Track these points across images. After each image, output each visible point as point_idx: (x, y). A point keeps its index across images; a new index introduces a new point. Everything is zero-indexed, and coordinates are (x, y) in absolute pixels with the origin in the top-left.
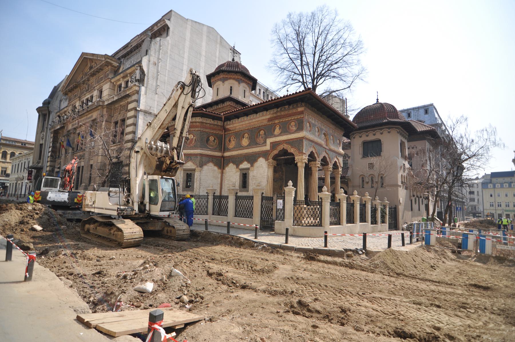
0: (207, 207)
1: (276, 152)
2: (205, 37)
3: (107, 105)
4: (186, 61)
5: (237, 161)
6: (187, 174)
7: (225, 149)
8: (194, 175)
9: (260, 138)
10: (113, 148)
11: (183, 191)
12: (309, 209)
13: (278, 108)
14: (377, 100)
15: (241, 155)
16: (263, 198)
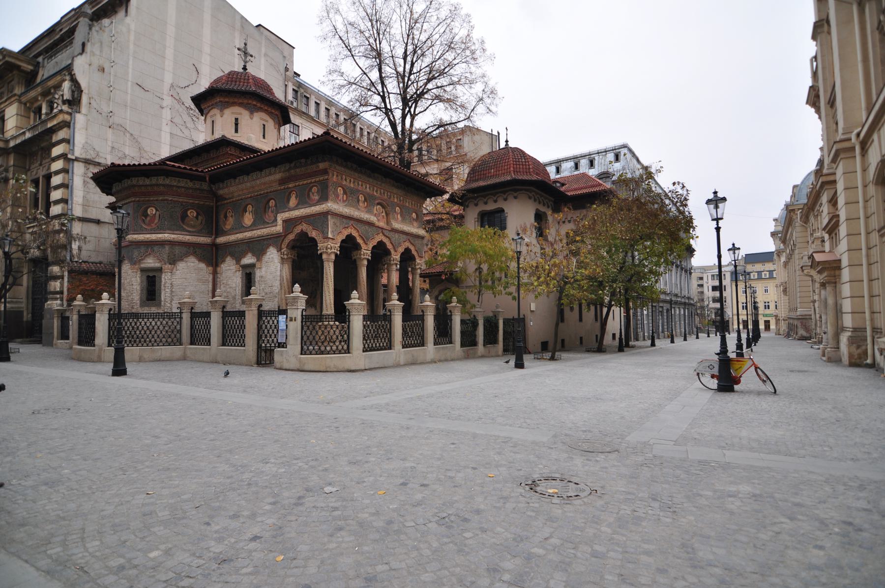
0: (180, 331)
1: (291, 237)
2: (207, 16)
3: (14, 147)
4: (169, 64)
5: (236, 250)
6: (148, 277)
7: (219, 232)
8: (160, 278)
9: (270, 214)
10: (31, 230)
11: (142, 305)
12: (343, 327)
13: (290, 162)
14: (507, 141)
15: (242, 240)
16: (261, 314)
